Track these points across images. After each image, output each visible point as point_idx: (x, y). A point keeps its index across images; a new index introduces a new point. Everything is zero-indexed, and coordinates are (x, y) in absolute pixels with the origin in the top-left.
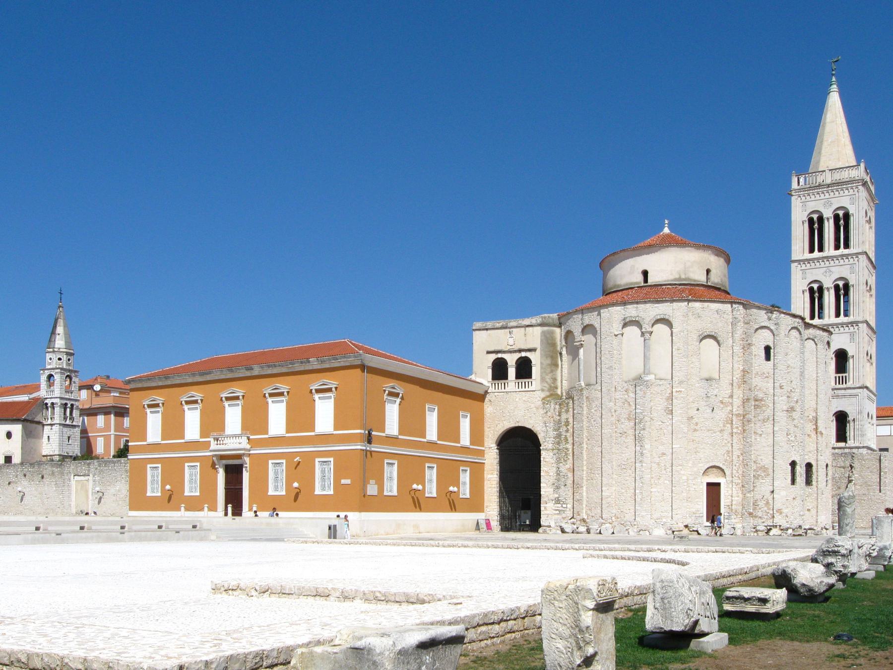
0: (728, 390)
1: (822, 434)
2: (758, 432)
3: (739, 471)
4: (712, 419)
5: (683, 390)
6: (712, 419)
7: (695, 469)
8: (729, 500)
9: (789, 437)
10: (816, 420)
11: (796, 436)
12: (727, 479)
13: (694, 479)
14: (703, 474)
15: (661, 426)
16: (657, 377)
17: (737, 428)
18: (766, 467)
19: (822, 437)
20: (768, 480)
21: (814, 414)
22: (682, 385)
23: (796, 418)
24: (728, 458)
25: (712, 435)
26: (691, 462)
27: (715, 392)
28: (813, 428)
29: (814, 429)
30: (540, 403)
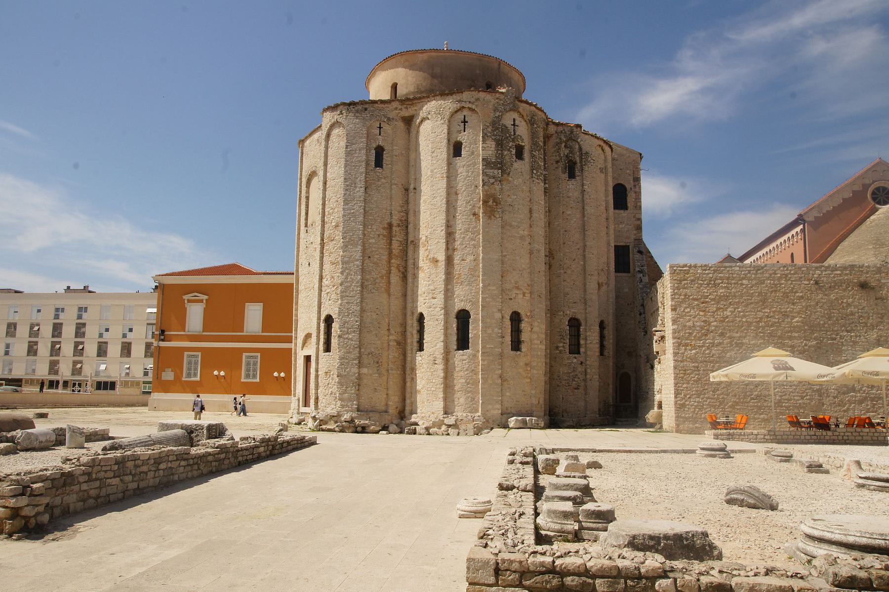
1: (437, 261)
19: (436, 267)
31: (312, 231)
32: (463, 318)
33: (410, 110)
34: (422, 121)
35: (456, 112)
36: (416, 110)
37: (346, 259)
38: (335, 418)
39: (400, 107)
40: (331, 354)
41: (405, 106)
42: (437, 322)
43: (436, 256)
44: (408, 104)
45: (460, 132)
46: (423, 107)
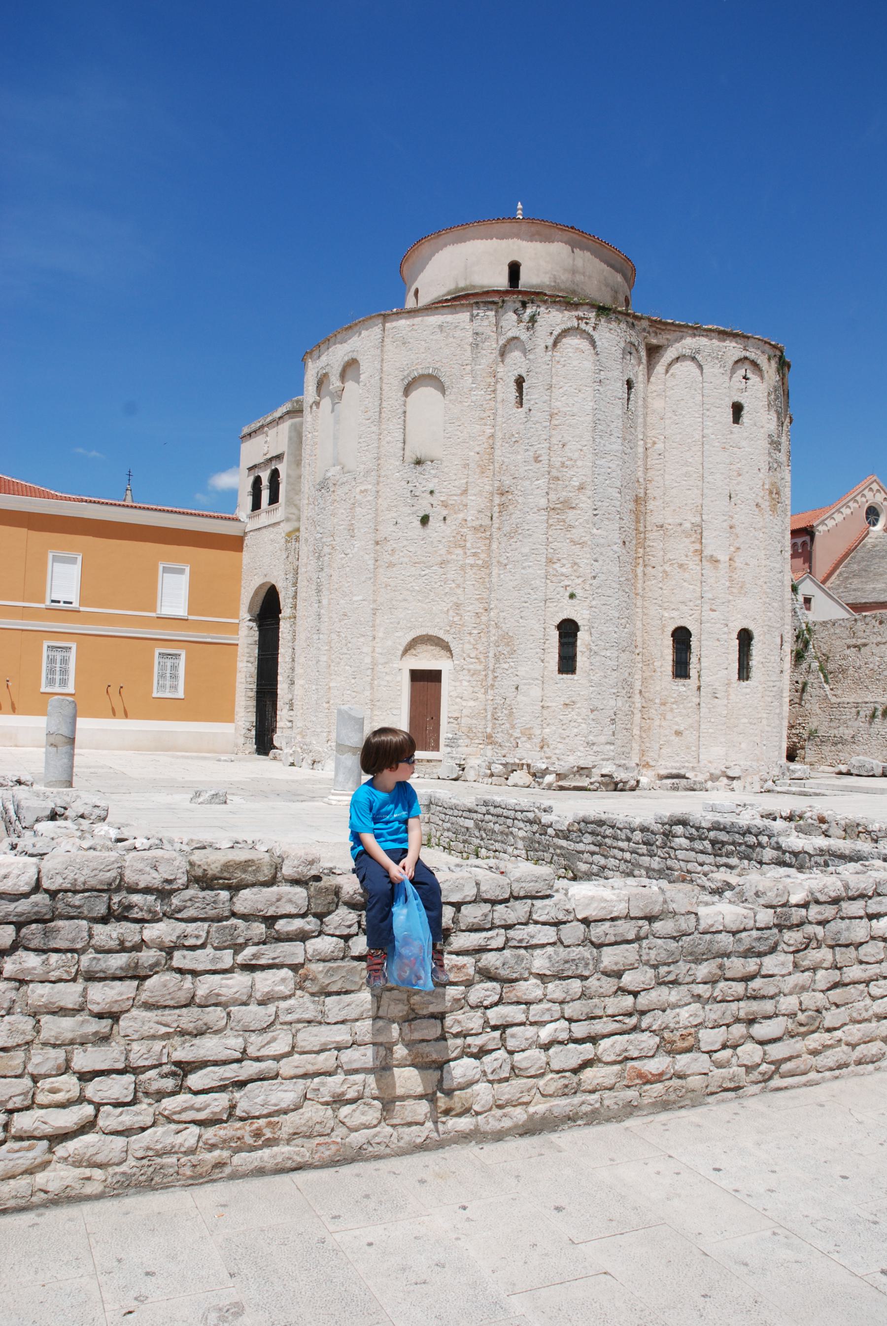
0: (460, 479)
2: (501, 559)
3: (478, 646)
4: (423, 539)
5: (370, 487)
6: (423, 539)
7: (389, 643)
8: (456, 707)
9: (555, 566)
10: (698, 530)
11: (575, 564)
12: (456, 662)
13: (386, 663)
14: (406, 651)
15: (343, 562)
16: (345, 470)
17: (475, 554)
18: (511, 634)
19: (716, 568)
20: (512, 664)
21: (697, 520)
22: (369, 479)
23: (577, 523)
24: (456, 619)
25: (424, 573)
26: (382, 629)
27: (431, 486)
28: (692, 549)
29: (696, 551)
30: (284, 540)
31: (433, 472)
32: (745, 638)
33: (660, 336)
34: (677, 359)
35: (737, 362)
36: (667, 339)
37: (602, 541)
38: (582, 770)
39: (648, 329)
40: (575, 677)
41: (654, 329)
42: (718, 643)
43: (715, 554)
44: (660, 329)
45: (742, 391)
46: (682, 338)
